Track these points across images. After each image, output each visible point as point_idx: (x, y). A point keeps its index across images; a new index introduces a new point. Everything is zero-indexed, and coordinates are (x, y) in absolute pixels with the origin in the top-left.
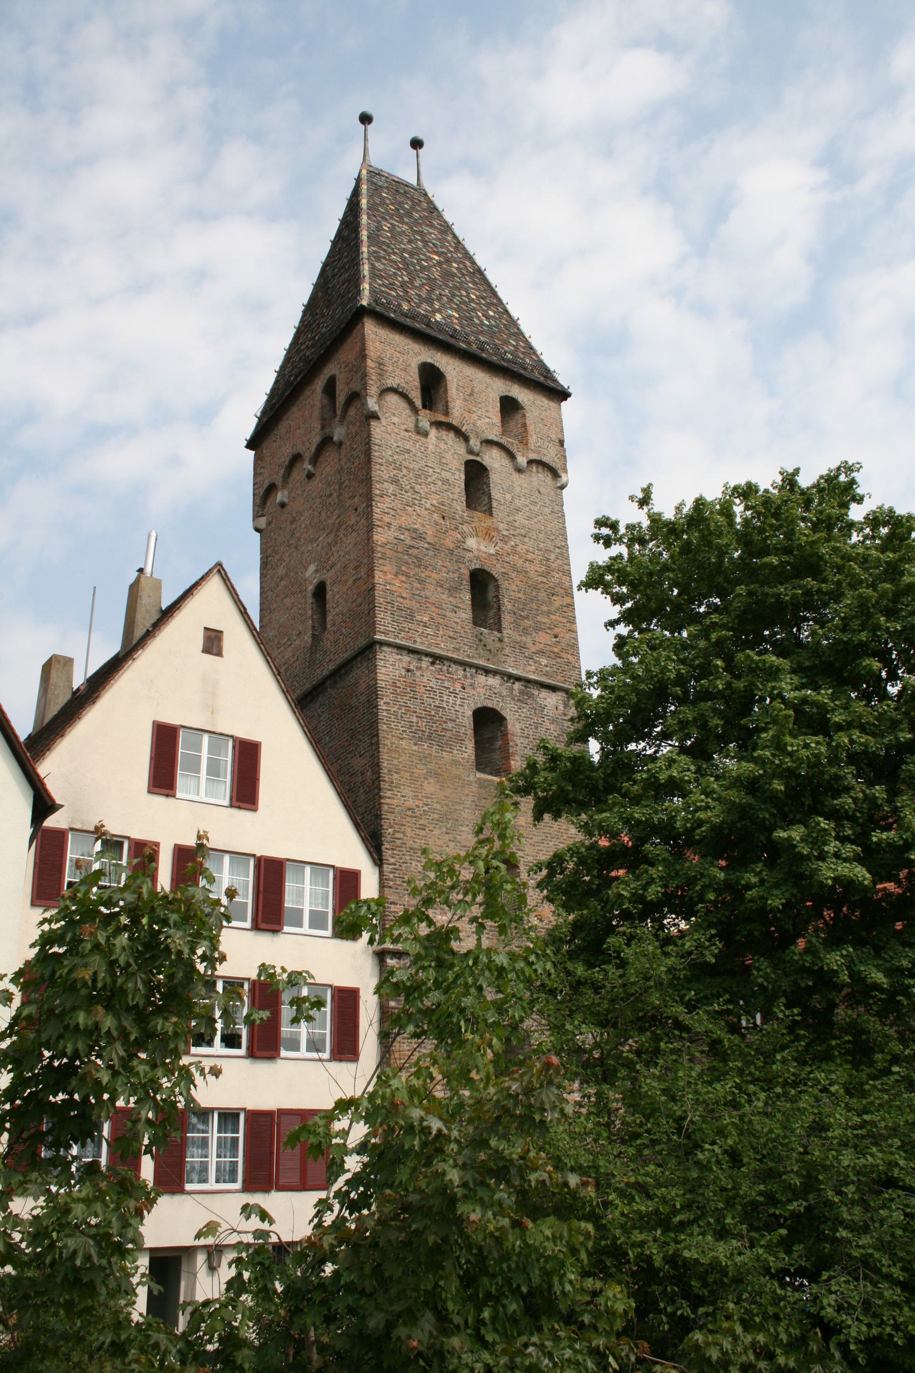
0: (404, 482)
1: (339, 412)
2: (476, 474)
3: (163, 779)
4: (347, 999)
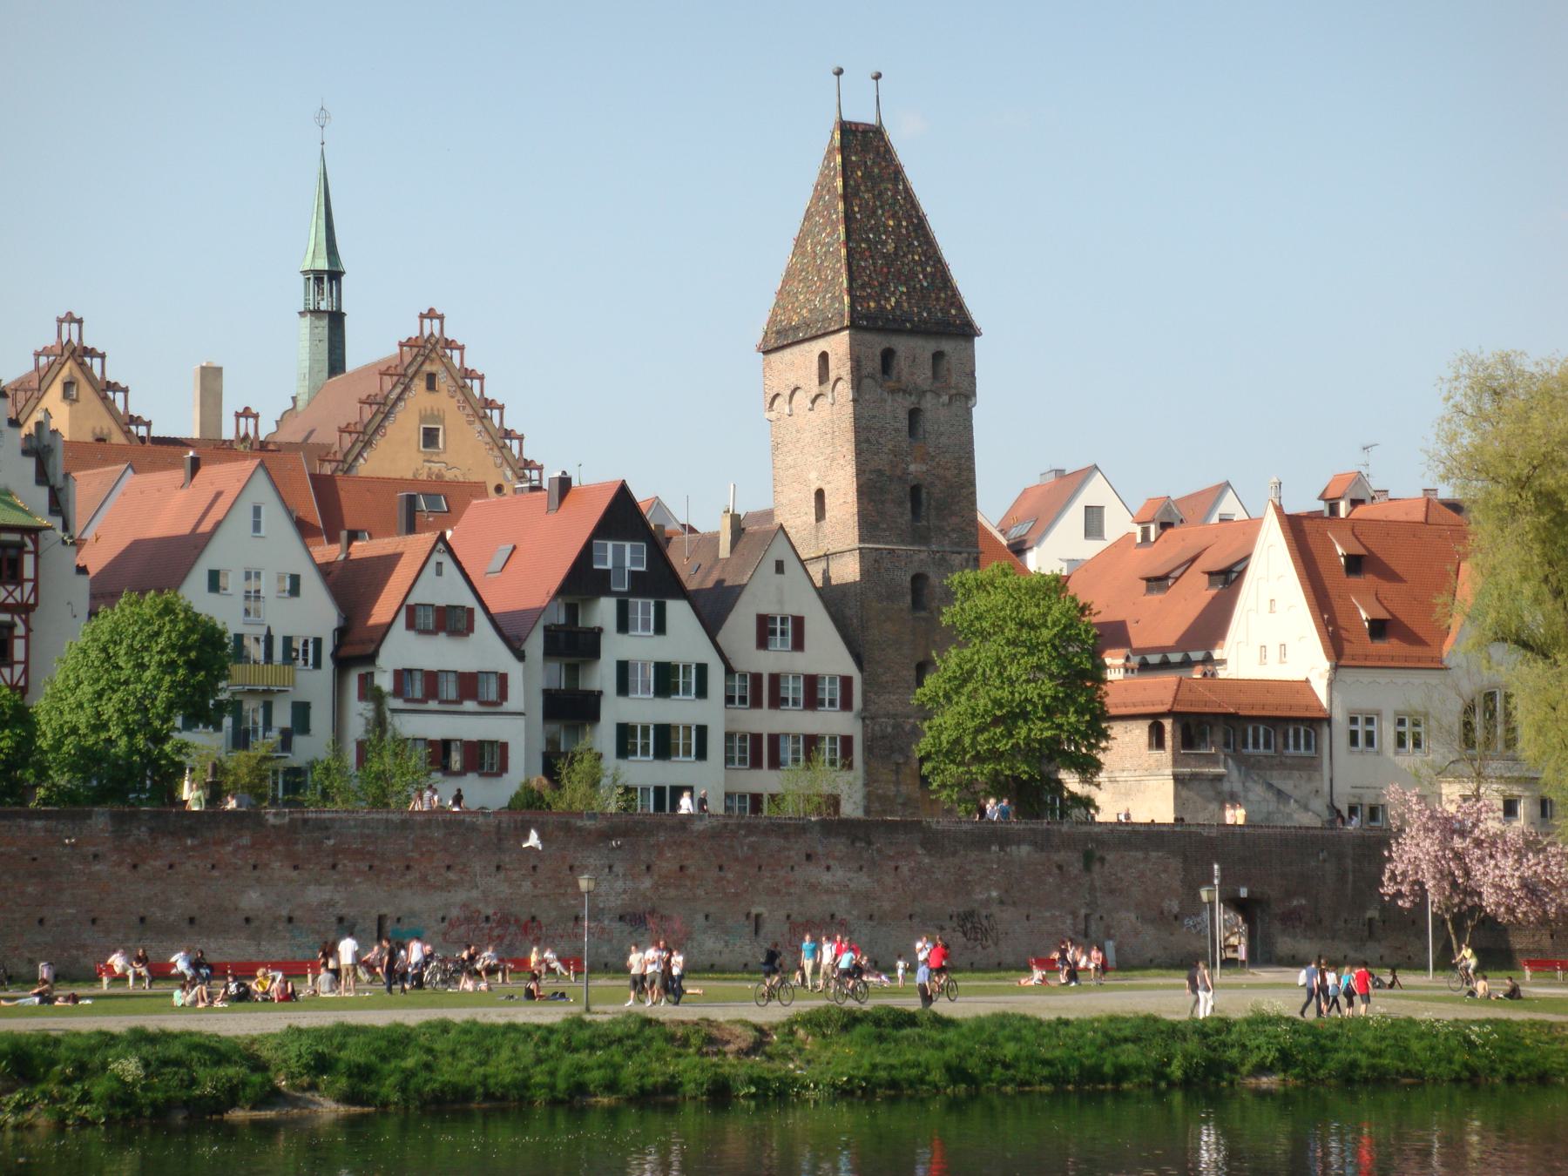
0: (873, 439)
1: (831, 382)
2: (914, 414)
3: (762, 643)
4: (847, 741)
